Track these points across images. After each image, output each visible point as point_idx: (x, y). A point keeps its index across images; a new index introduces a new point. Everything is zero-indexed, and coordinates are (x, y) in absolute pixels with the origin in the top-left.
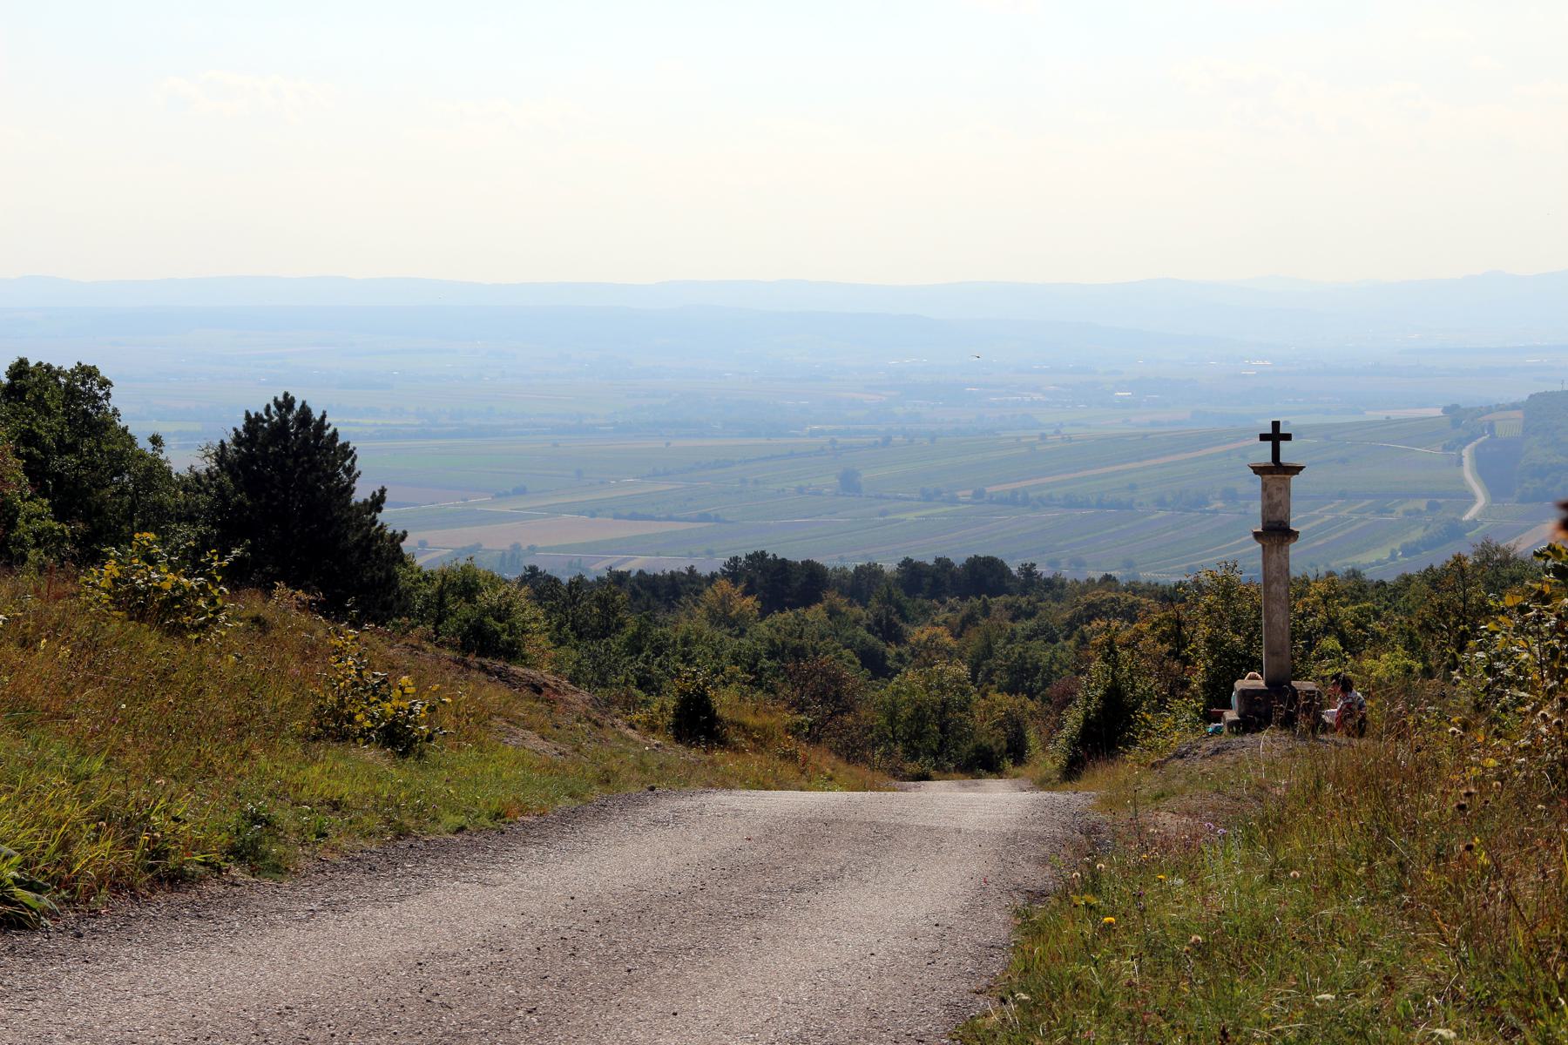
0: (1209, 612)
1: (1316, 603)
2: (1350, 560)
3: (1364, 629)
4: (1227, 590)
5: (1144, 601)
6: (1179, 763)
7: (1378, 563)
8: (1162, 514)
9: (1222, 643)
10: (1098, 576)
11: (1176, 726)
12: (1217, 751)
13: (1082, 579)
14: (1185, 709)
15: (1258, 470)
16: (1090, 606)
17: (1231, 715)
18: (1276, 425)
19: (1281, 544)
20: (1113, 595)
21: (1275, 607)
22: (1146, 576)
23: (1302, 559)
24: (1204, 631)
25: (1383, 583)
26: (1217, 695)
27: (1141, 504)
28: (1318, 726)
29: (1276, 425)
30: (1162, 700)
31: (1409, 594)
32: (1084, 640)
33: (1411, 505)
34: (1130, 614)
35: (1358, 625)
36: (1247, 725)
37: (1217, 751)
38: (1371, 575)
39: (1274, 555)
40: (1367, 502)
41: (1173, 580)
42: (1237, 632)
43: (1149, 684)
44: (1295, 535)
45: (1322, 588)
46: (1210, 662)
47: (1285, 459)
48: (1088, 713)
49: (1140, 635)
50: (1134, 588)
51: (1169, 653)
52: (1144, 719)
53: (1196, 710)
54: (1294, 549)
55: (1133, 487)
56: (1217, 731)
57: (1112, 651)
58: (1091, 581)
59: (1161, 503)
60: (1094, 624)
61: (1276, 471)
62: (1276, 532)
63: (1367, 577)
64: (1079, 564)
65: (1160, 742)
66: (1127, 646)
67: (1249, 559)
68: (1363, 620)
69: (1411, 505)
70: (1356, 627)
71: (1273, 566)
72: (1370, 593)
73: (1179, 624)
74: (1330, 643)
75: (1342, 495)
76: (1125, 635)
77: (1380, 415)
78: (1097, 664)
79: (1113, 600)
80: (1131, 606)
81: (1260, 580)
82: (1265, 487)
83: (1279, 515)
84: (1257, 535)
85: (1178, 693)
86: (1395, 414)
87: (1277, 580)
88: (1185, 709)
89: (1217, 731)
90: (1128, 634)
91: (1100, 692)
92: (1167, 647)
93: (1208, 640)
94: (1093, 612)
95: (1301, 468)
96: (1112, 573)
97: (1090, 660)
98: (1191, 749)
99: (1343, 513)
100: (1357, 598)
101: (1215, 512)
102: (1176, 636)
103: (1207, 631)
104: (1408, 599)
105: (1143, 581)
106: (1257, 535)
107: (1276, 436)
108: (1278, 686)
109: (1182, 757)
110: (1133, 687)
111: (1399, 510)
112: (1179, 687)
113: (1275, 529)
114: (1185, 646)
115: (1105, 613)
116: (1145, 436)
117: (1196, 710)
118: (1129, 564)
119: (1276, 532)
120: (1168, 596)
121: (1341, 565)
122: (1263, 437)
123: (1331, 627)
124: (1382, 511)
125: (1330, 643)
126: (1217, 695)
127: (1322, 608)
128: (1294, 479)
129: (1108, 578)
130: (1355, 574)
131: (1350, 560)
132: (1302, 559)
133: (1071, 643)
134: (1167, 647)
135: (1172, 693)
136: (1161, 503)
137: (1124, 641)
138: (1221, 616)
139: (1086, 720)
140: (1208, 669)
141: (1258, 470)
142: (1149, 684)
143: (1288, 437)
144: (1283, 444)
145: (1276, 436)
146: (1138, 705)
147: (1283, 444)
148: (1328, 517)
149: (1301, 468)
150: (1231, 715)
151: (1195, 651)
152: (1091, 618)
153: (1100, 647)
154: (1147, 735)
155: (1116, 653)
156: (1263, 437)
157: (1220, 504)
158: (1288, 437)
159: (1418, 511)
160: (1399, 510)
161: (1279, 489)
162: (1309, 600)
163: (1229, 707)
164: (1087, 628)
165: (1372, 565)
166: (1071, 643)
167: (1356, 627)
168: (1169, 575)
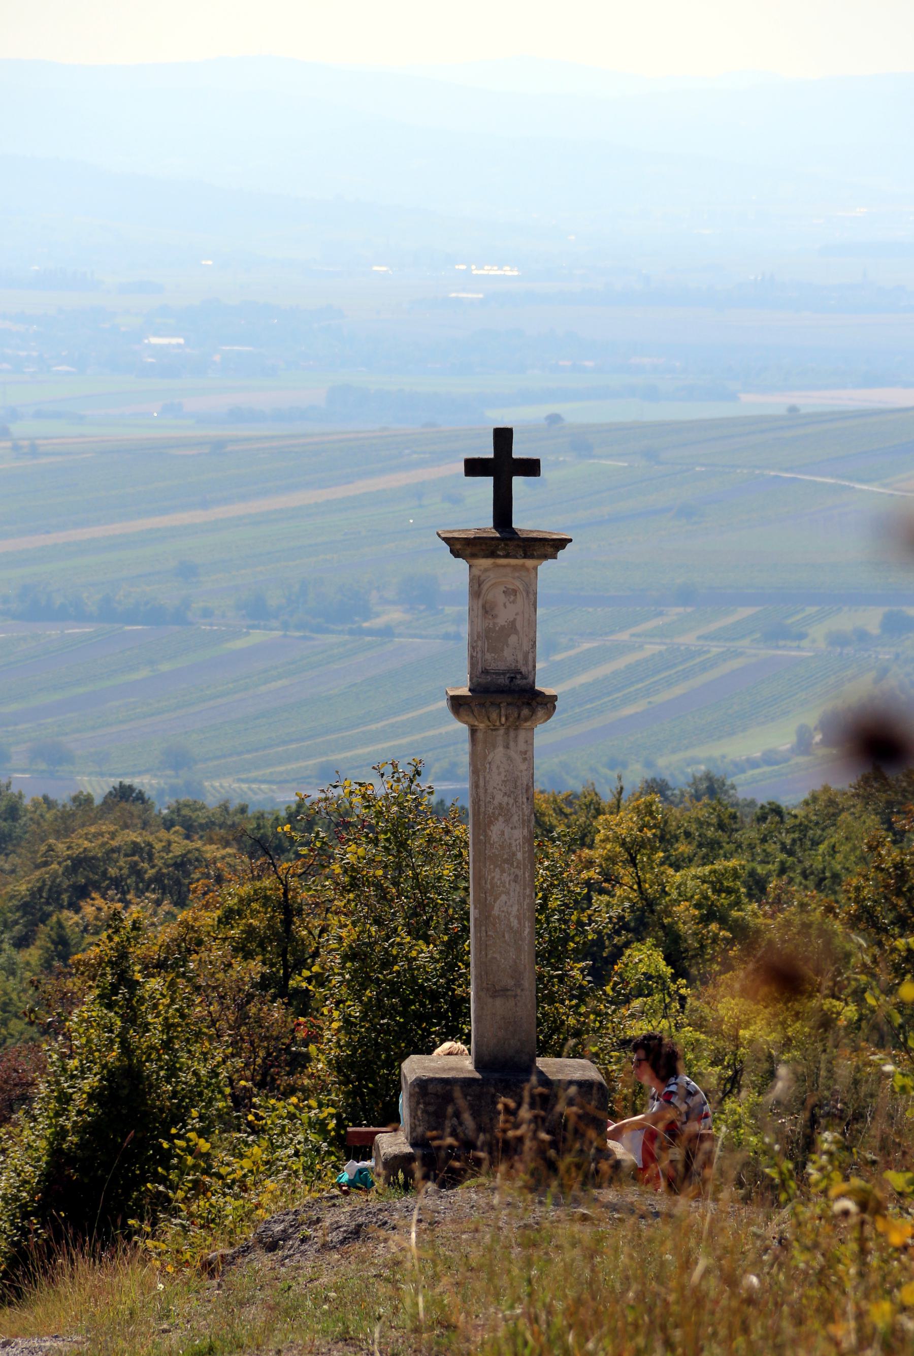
0: (354, 885)
1: (611, 859)
2: (701, 752)
3: (723, 921)
4: (399, 826)
5: (212, 851)
6: (263, 1261)
7: (769, 759)
8: (257, 637)
9: (387, 963)
10: (98, 788)
11: (264, 1171)
12: (357, 1233)
13: (62, 797)
14: (296, 1120)
15: (462, 547)
16: (79, 863)
17: (392, 1143)
18: (503, 437)
19: (515, 725)
20: (133, 836)
21: (498, 876)
22: (220, 788)
23: (562, 755)
24: (342, 932)
25: (777, 811)
26: (369, 1093)
27: (207, 613)
28: (598, 1171)
29: (503, 437)
30: (240, 1101)
31: (836, 836)
32: (62, 946)
33: (845, 621)
34: (174, 884)
35: (710, 914)
36: (437, 1164)
37: (357, 1233)
38: (751, 788)
39: (498, 754)
40: (745, 612)
41: (285, 798)
42: (420, 933)
43: (210, 1062)
44: (548, 703)
45: (625, 824)
46: (356, 1011)
47: (524, 521)
48: (62, 1133)
49: (190, 943)
50: (186, 820)
51: (264, 983)
52: (190, 1150)
53: (320, 1126)
54: (545, 735)
55: (187, 571)
56: (361, 1182)
57: (124, 979)
58: (82, 801)
59: (257, 611)
60: (89, 910)
61: (504, 546)
62: (504, 697)
63: (742, 794)
64: (54, 756)
65: (230, 1207)
66: (161, 965)
67: (446, 756)
68: (724, 900)
69: (845, 621)
70: (705, 920)
71: (496, 779)
72: (749, 833)
73: (289, 910)
74: (645, 958)
75: (686, 596)
76: (162, 935)
77: (774, 403)
78: (88, 1008)
79: (136, 849)
80: (182, 864)
81: (468, 805)
82: (477, 588)
83: (508, 657)
84: (457, 704)
85: (284, 1081)
86: (813, 401)
87: (504, 812)
88: (296, 1120)
89: (361, 1182)
90: (166, 933)
91: (90, 1082)
92: (256, 968)
93: (351, 956)
94: (86, 877)
95: (562, 543)
96: (137, 782)
97: (69, 1001)
98: (297, 1226)
99: (688, 640)
100: (714, 845)
101: (387, 632)
102: (281, 940)
103: (349, 934)
104: (833, 850)
105: (211, 801)
106: (457, 704)
107: (502, 464)
108: (504, 1070)
109: (272, 1247)
110: (173, 1071)
111: (818, 632)
112: (278, 1068)
113: (501, 691)
114: (300, 964)
115: (117, 883)
116: (219, 446)
117: (320, 1126)
118: (177, 759)
119: (504, 697)
120: (263, 845)
121: (680, 766)
122: (474, 467)
123: (645, 920)
124: (778, 634)
125: (645, 958)
126: (369, 1093)
127: (626, 874)
128: (547, 571)
129: (124, 793)
130: (712, 788)
131: (701, 752)
132: (562, 755)
133: (33, 955)
134: (256, 968)
135: (266, 1083)
136: (257, 611)
137: (155, 953)
138: (383, 896)
139: (56, 1153)
140: (348, 1022)
141: (462, 547)
142: (210, 1062)
143: (531, 467)
144: (519, 483)
145: (502, 464)
146: (179, 1117)
147: (519, 483)
148: (652, 649)
149: (562, 543)
150: (392, 1143)
151: (320, 980)
152: (82, 893)
153: (92, 971)
154: (199, 1188)
155: (133, 985)
156: (474, 467)
157: (394, 615)
158: (531, 467)
159: (862, 636)
160: (818, 632)
161: (511, 593)
162: (597, 854)
163: (390, 1118)
164: (70, 918)
165: (754, 764)
166: (33, 955)
167: (705, 920)
168: (269, 788)
